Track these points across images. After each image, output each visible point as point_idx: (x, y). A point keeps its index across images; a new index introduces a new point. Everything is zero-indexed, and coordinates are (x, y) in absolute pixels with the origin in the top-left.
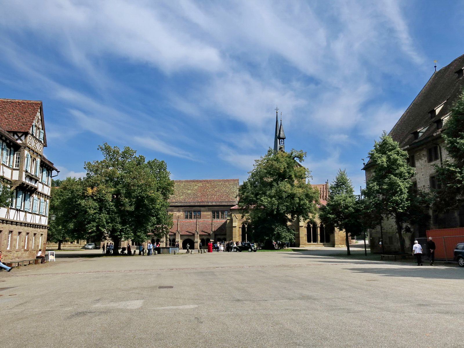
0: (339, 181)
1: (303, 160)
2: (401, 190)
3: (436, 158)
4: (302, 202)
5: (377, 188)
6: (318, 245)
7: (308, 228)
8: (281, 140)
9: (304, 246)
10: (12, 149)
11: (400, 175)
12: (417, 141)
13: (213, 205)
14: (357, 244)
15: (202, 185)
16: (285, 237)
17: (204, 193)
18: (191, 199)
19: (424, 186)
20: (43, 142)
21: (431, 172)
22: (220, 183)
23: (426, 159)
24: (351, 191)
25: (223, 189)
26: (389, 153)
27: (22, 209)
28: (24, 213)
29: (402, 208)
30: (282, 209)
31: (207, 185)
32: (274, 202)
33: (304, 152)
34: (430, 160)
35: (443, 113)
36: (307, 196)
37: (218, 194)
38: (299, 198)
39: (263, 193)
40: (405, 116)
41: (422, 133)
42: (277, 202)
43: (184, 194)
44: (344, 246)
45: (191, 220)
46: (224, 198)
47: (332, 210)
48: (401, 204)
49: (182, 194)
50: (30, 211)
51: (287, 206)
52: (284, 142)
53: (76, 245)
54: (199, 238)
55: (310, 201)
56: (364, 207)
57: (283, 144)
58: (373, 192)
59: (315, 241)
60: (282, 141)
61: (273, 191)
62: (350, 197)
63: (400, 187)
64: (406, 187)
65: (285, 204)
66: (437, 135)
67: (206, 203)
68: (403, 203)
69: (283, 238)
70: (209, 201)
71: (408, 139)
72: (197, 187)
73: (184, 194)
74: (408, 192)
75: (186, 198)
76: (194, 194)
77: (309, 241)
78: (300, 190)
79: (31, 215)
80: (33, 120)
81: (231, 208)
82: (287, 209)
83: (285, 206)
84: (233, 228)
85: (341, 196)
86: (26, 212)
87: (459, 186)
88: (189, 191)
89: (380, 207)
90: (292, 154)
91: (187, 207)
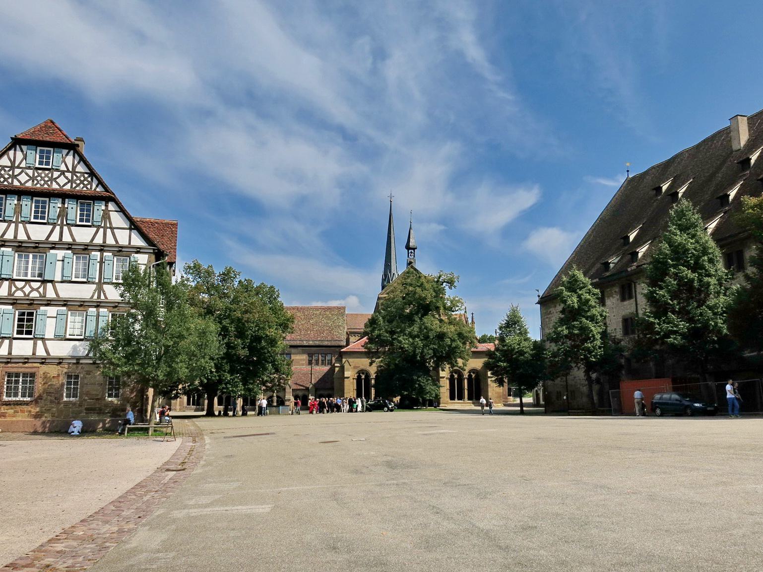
0: (511, 319)
1: (455, 287)
2: (593, 336)
3: (630, 297)
4: (454, 345)
5: (566, 332)
6: (465, 403)
7: (451, 380)
8: (410, 251)
9: (446, 405)
11: (592, 318)
12: (608, 274)
14: (515, 402)
16: (429, 392)
19: (615, 329)
21: (623, 313)
22: (318, 312)
23: (618, 297)
24: (526, 333)
26: (580, 292)
29: (595, 356)
30: (428, 353)
31: (298, 315)
32: (418, 344)
33: (456, 275)
34: (623, 299)
35: (639, 241)
36: (460, 335)
38: (450, 338)
39: (401, 332)
40: (591, 235)
41: (614, 264)
42: (422, 344)
44: (500, 405)
46: (325, 334)
47: (503, 356)
48: (593, 351)
51: (434, 349)
52: (414, 253)
55: (464, 343)
56: (552, 354)
57: (413, 257)
58: (562, 337)
59: (461, 397)
60: (411, 252)
61: (415, 329)
62: (525, 340)
63: (592, 333)
64: (599, 333)
65: (432, 346)
66: (631, 270)
68: (595, 351)
69: (428, 393)
70: (303, 339)
71: (596, 269)
74: (601, 338)
77: (452, 397)
78: (452, 328)
81: (342, 350)
82: (434, 353)
83: (431, 349)
84: (345, 380)
85: (512, 340)
87: (657, 337)
89: (572, 355)
90: (439, 277)
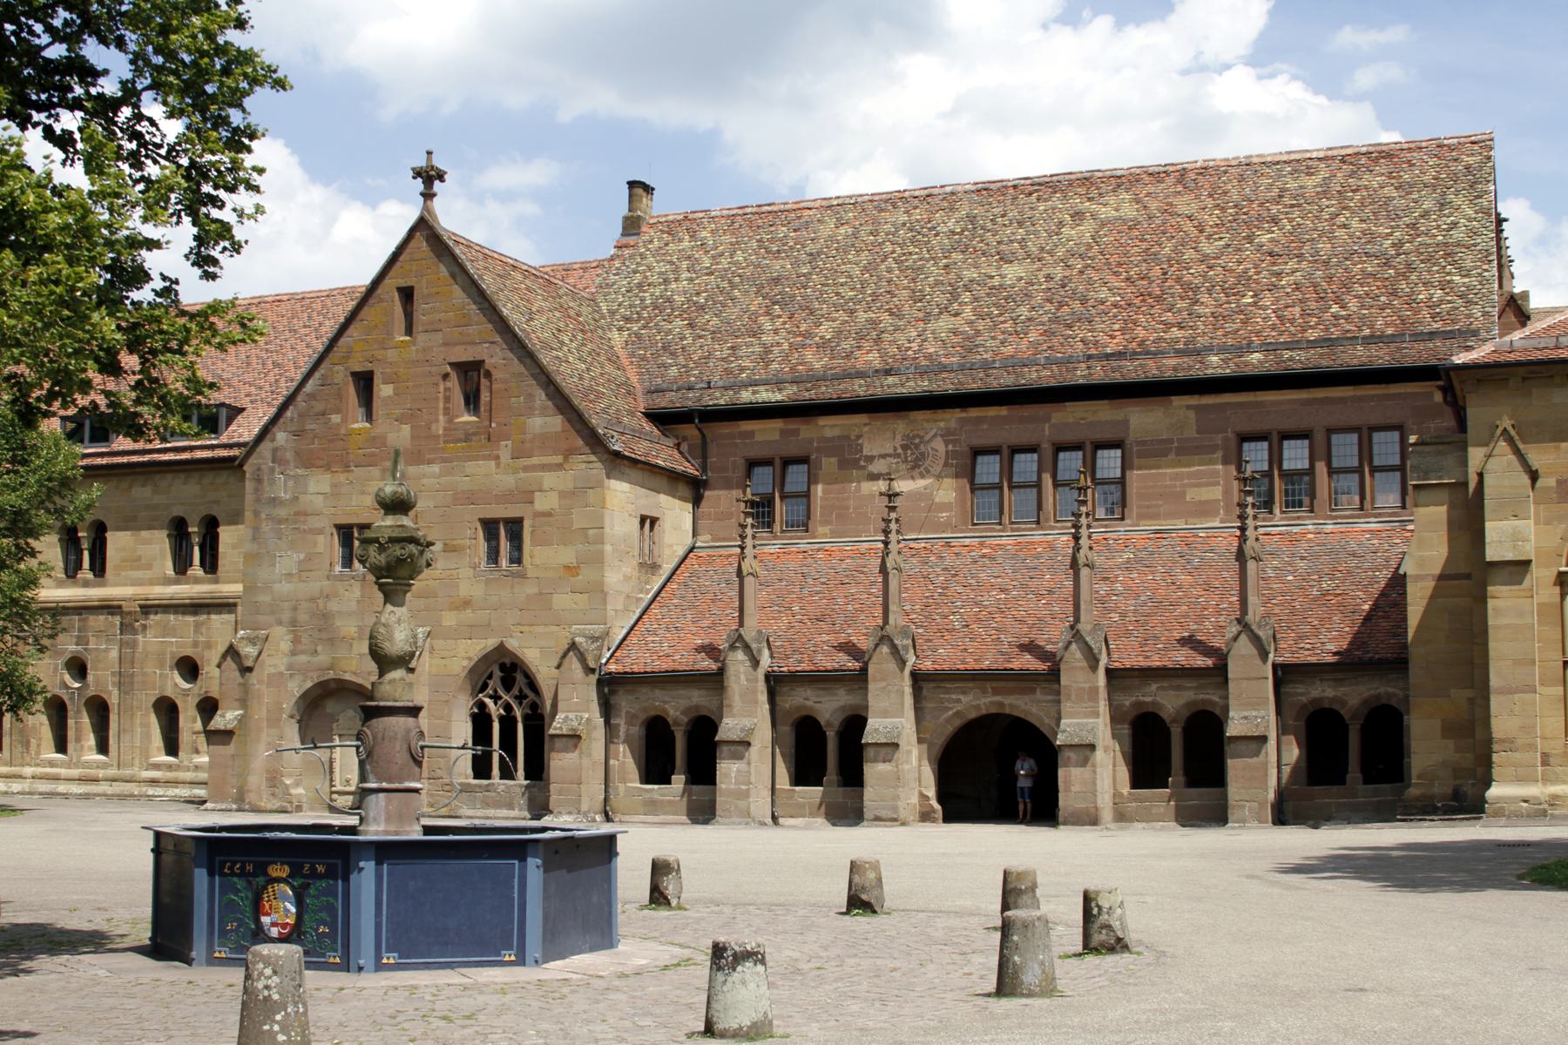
13: (1248, 371)
15: (1129, 211)
17: (1157, 271)
18: (1033, 336)
22: (1310, 182)
25: (1340, 233)
31: (1182, 209)
37: (1294, 272)
43: (967, 297)
45: (1037, 536)
46: (1353, 305)
49: (942, 299)
53: (88, 765)
54: (1103, 707)
67: (1173, 362)
70: (1202, 341)
72: (1087, 228)
75: (978, 333)
76: (1058, 293)
88: (1012, 272)
91: (992, 412)
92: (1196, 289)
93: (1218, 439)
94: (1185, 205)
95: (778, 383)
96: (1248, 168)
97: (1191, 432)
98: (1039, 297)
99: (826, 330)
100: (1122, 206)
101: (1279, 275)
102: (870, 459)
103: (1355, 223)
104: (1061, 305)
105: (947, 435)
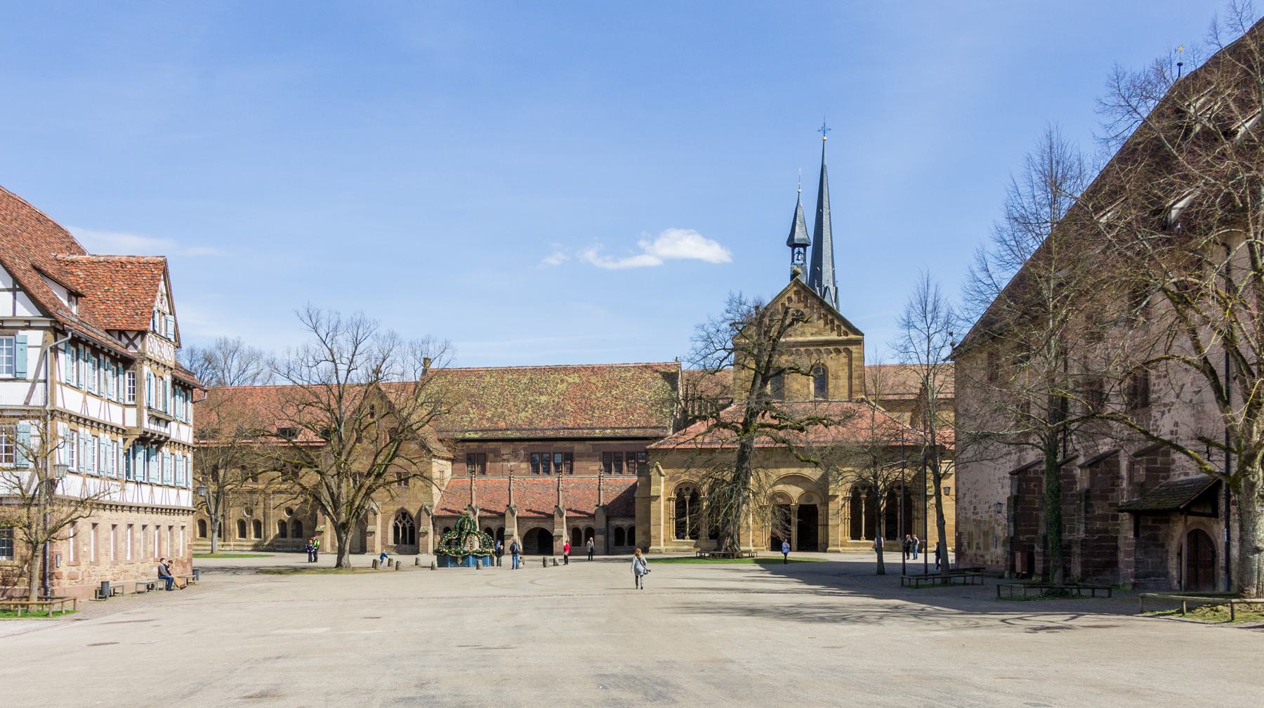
10: (120, 365)
13: (606, 436)
15: (577, 380)
18: (549, 420)
20: (173, 340)
22: (629, 375)
27: (145, 481)
28: (149, 487)
31: (593, 381)
43: (530, 406)
45: (549, 478)
46: (636, 416)
49: (522, 406)
50: (159, 483)
72: (565, 385)
73: (530, 406)
76: (557, 406)
79: (160, 489)
80: (153, 301)
81: (648, 447)
86: (151, 484)
88: (543, 399)
92: (594, 408)
93: (598, 453)
94: (593, 379)
95: (476, 431)
96: (612, 368)
97: (591, 451)
98: (551, 408)
99: (489, 414)
100: (574, 378)
101: (617, 405)
102: (503, 455)
103: (639, 389)
104: (557, 411)
105: (525, 449)
